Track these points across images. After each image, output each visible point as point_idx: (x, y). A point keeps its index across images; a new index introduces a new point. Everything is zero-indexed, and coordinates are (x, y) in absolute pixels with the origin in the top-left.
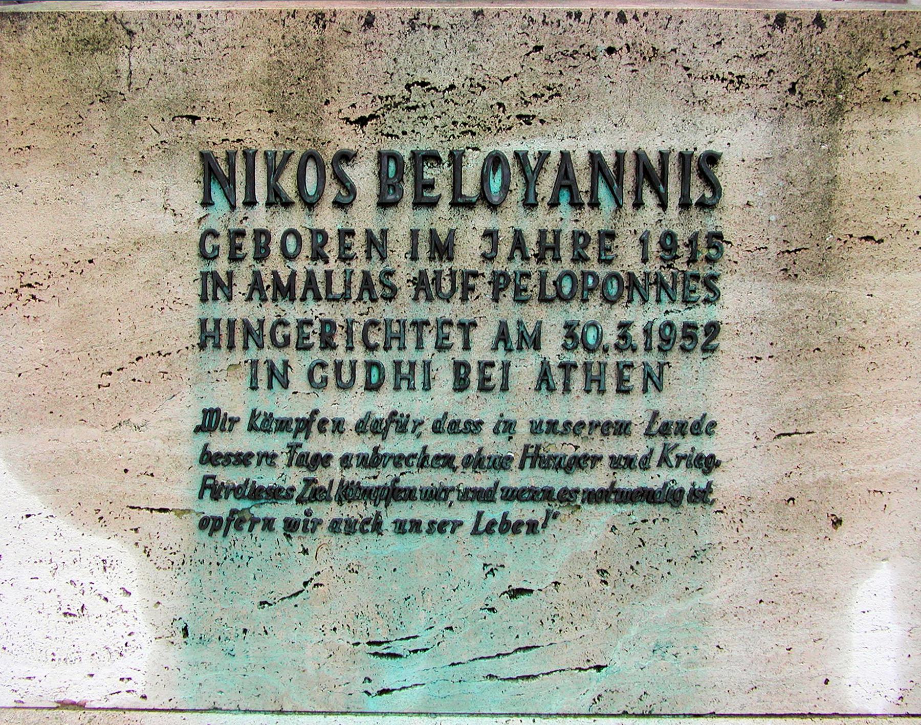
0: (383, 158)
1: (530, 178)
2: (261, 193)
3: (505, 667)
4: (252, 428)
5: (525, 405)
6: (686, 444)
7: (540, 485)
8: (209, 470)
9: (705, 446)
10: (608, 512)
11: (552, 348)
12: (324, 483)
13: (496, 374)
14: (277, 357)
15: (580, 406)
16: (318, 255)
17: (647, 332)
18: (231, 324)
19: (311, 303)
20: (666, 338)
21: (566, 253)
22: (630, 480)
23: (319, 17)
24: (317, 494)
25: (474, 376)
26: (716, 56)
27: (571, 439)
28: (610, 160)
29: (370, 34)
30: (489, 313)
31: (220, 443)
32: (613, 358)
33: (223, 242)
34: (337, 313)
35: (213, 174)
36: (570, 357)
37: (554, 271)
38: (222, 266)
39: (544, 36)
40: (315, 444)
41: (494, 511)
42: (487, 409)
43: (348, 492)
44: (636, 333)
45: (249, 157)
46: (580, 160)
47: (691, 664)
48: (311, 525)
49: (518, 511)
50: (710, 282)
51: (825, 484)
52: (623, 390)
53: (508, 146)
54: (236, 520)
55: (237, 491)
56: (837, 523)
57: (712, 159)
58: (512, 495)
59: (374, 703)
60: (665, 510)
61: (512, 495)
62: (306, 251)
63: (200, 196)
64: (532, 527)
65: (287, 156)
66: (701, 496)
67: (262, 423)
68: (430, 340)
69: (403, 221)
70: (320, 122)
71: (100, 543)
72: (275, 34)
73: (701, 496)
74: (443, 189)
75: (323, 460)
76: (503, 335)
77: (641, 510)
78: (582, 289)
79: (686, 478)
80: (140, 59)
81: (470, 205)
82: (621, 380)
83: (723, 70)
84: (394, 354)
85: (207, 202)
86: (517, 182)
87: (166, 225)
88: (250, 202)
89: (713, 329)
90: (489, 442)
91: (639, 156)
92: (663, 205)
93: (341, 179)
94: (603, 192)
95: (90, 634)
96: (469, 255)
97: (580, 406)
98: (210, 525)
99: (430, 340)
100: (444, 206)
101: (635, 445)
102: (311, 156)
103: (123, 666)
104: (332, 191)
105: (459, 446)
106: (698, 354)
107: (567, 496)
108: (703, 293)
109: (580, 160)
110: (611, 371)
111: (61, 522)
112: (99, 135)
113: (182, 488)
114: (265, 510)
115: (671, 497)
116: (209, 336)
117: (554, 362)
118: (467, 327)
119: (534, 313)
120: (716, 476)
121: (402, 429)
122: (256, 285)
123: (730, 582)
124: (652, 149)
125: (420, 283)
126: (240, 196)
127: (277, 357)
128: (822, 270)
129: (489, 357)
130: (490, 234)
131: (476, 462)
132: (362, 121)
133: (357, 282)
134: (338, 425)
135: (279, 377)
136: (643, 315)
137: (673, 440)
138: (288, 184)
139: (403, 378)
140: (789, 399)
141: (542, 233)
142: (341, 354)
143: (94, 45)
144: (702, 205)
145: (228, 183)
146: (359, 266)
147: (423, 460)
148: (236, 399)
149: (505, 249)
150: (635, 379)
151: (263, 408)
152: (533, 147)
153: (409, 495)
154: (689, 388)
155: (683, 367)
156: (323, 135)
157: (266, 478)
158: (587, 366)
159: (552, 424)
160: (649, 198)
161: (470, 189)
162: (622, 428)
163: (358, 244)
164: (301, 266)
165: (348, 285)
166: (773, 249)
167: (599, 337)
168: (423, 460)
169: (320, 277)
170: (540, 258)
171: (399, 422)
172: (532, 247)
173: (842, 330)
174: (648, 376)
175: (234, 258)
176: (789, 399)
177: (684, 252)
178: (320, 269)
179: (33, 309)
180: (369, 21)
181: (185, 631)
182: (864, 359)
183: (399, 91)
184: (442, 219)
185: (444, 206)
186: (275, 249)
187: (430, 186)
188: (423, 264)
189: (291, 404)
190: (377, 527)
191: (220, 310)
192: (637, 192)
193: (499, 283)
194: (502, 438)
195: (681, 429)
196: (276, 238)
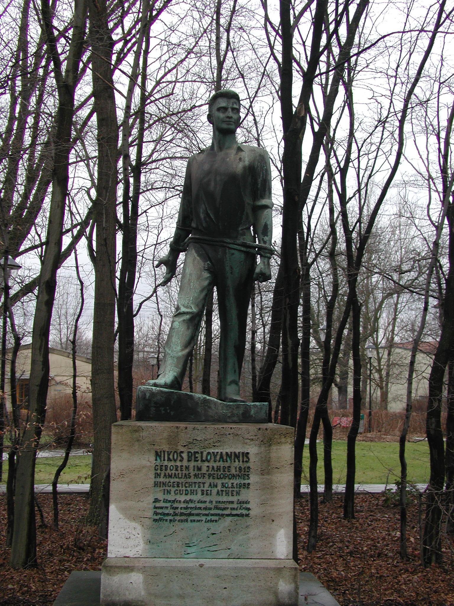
0: (189, 452)
1: (215, 456)
2: (166, 458)
3: (212, 549)
4: (164, 502)
5: (214, 498)
6: (245, 506)
7: (218, 512)
8: (155, 510)
9: (248, 506)
10: (230, 518)
11: (219, 488)
12: (177, 512)
13: (209, 492)
14: (169, 488)
15: (225, 498)
16: (177, 470)
17: (237, 484)
18: (160, 482)
19: (175, 479)
20: (240, 486)
21: (222, 470)
22: (234, 512)
23: (177, 427)
24: (176, 514)
25: (205, 492)
26: (248, 435)
27: (223, 504)
28: (229, 453)
29: (186, 431)
30: (208, 481)
31: (158, 505)
32: (231, 489)
33: (159, 467)
34: (180, 481)
35: (158, 455)
36: (223, 489)
37: (220, 473)
38: (159, 471)
39: (217, 431)
40: (175, 505)
41: (209, 518)
42: (208, 499)
43: (182, 514)
44: (235, 484)
45: (164, 452)
46: (224, 453)
47: (247, 548)
48: (174, 521)
49: (214, 518)
50: (248, 475)
51: (270, 513)
52: (232, 495)
53: (211, 451)
54: (160, 520)
55: (161, 514)
56: (273, 521)
57: (248, 453)
58: (212, 515)
59: (186, 556)
60: (241, 518)
61: (212, 515)
62: (174, 469)
63: (155, 459)
64: (216, 521)
65: (171, 452)
66: (247, 515)
67: (165, 501)
68: (197, 486)
69: (192, 464)
70: (177, 446)
71: (134, 524)
72: (169, 430)
73: (247, 515)
74: (199, 458)
75: (177, 508)
76: (210, 485)
77: (236, 518)
78: (225, 477)
79: (244, 512)
80: (144, 434)
81: (204, 461)
82: (232, 493)
83: (250, 438)
84: (190, 488)
85: (156, 460)
86: (213, 457)
87: (149, 464)
88: (164, 460)
89: (249, 484)
90: (208, 505)
91: (235, 453)
92: (239, 462)
93: (181, 456)
94: (228, 459)
95: (131, 543)
96: (204, 470)
97: (225, 498)
98: (155, 520)
99: (197, 486)
100: (199, 462)
101: (235, 506)
102: (175, 452)
103: (137, 549)
104: (179, 458)
105: (202, 505)
106: (246, 489)
107: (222, 515)
108: (247, 478)
109: (224, 453)
110: (230, 492)
111: (126, 520)
112: (136, 447)
113: (150, 514)
114: (166, 518)
115: (242, 515)
116: (156, 484)
117: (220, 490)
118: (204, 483)
119: (216, 481)
120: (250, 512)
121: (192, 502)
122: (165, 475)
123: (253, 532)
124: (237, 451)
125: (195, 475)
126: (162, 459)
127: (169, 488)
128: (268, 473)
129: (208, 489)
130: (208, 466)
131: (205, 509)
132: (185, 446)
133: (184, 475)
134: (180, 501)
135: (169, 492)
136: (236, 481)
137: (242, 505)
138: (171, 457)
139: (192, 492)
140: (263, 497)
141: (217, 466)
142: (180, 488)
143: (136, 431)
144: (246, 462)
145: (160, 456)
146: (184, 472)
147: (196, 508)
148: (161, 496)
149: (210, 469)
150: (235, 493)
151: (166, 498)
152: (217, 451)
153: (193, 515)
154: (245, 495)
155: (243, 491)
156: (178, 448)
157: (166, 511)
158: (226, 491)
159: (220, 501)
160: (237, 460)
161: (204, 458)
162: (232, 502)
163: (184, 468)
164: (173, 472)
165: (182, 475)
166: (259, 470)
167: (228, 485)
168: (196, 508)
169: (177, 474)
170: (217, 471)
171: (191, 501)
172: (216, 469)
173: (273, 485)
174: (237, 493)
175: (161, 470)
176: (263, 497)
177: (243, 470)
178: (177, 472)
179: (123, 479)
180: (186, 428)
181: (150, 542)
182: (277, 490)
183: (191, 441)
184: (199, 463)
185: (199, 462)
186: (169, 469)
187: (197, 458)
188: (196, 472)
189: (171, 497)
190: (187, 521)
191: (158, 480)
192: (234, 459)
193: (210, 475)
194: (210, 504)
195: (243, 503)
196: (169, 467)
